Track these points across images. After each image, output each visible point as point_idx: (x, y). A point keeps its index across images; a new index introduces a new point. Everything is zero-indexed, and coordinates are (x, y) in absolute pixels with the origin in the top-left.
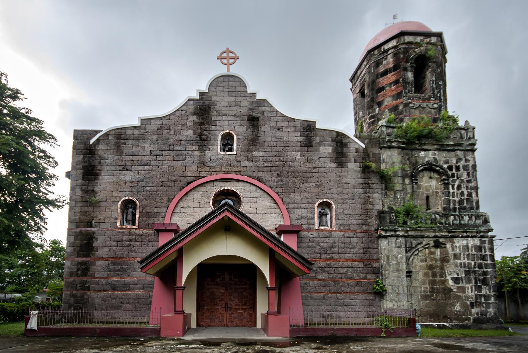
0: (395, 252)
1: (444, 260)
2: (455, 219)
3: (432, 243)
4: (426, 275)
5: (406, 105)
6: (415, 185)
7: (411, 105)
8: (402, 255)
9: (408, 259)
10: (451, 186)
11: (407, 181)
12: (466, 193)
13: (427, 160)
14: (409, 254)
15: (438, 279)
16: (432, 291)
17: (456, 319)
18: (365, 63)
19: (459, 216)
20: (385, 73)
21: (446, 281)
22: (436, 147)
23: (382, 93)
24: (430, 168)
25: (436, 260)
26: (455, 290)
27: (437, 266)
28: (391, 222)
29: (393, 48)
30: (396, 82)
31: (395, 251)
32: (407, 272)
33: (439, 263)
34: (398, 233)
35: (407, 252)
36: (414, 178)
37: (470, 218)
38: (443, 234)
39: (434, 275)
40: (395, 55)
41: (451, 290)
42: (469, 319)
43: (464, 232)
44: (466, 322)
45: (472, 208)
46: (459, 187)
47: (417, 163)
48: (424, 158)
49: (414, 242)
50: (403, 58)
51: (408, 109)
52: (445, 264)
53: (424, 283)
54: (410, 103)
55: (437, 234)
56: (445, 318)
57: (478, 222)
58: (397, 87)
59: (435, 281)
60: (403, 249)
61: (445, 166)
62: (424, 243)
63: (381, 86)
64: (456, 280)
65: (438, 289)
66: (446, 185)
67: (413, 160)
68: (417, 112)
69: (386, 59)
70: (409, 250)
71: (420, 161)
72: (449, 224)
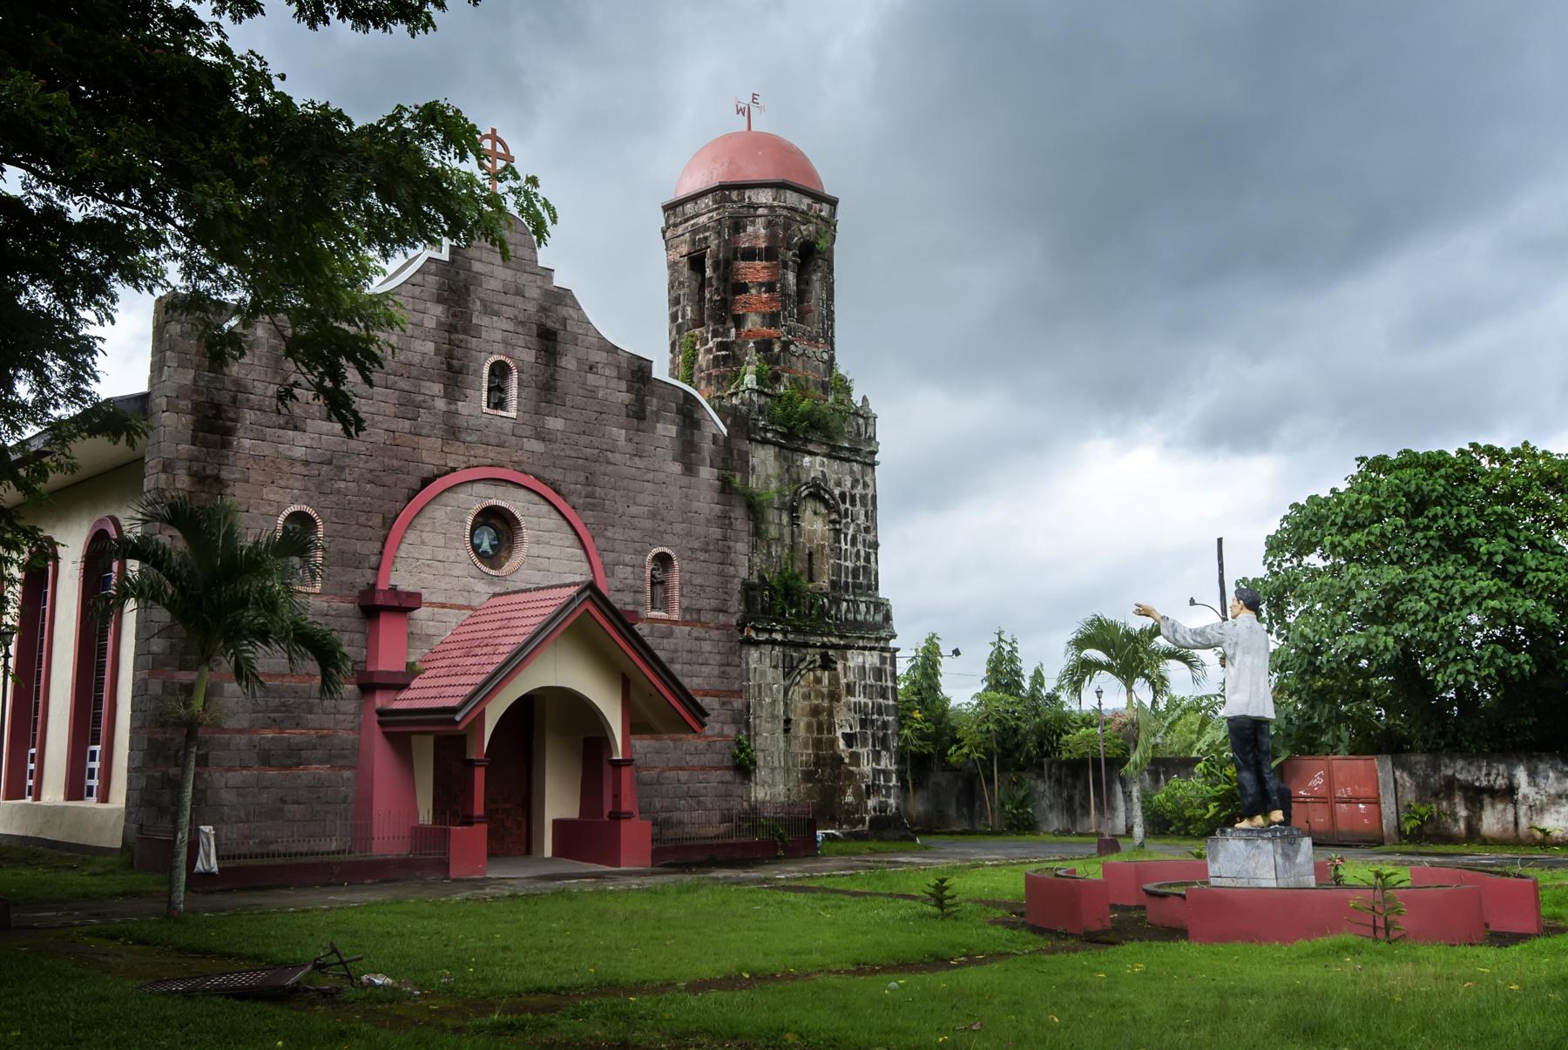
0: (769, 680)
1: (834, 696)
2: (848, 610)
4: (809, 727)
11: (785, 519)
12: (862, 553)
15: (825, 736)
16: (818, 761)
18: (708, 201)
20: (750, 255)
22: (824, 449)
23: (742, 297)
24: (818, 492)
30: (770, 287)
31: (770, 672)
33: (826, 704)
35: (786, 675)
38: (833, 640)
39: (820, 730)
40: (770, 225)
42: (862, 820)
45: (869, 587)
46: (854, 539)
47: (799, 480)
53: (806, 747)
54: (791, 342)
58: (772, 299)
61: (837, 492)
64: (849, 739)
69: (753, 223)
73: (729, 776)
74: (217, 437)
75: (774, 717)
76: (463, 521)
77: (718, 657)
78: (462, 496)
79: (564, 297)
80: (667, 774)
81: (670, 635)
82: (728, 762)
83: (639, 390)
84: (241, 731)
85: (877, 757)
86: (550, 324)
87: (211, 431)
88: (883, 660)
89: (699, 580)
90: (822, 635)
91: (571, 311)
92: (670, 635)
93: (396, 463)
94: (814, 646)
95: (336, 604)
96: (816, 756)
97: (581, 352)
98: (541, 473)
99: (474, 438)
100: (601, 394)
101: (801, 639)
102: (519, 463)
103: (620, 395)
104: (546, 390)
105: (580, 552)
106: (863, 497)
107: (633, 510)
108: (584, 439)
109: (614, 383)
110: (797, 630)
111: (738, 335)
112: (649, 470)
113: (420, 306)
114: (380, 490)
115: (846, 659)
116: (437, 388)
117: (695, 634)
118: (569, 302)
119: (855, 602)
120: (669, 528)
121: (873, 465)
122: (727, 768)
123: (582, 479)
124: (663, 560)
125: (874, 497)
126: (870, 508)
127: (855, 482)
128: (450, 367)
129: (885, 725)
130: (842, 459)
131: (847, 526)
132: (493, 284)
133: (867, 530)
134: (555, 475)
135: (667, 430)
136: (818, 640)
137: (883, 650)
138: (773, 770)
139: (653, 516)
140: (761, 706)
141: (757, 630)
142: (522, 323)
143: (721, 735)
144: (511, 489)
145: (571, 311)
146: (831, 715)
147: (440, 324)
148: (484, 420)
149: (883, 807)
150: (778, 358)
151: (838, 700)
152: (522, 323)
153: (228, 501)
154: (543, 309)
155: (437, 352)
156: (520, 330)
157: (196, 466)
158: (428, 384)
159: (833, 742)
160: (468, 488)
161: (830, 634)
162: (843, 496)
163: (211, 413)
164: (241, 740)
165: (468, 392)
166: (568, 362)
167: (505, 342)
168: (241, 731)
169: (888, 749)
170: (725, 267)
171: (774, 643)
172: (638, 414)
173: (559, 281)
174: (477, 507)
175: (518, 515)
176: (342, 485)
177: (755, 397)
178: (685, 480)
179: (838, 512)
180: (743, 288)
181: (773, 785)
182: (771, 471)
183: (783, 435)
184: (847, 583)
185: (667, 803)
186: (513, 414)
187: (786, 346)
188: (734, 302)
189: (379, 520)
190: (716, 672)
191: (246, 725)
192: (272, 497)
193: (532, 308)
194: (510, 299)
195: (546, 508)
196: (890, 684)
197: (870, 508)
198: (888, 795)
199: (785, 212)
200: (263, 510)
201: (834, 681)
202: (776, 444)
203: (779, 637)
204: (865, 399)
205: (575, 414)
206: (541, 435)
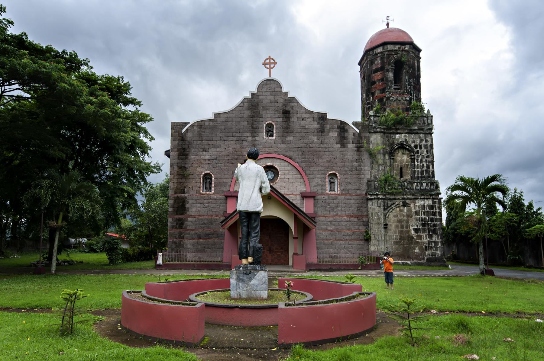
0: (377, 211)
2: (417, 185)
3: (401, 204)
4: (397, 227)
5: (388, 99)
6: (392, 160)
7: (391, 98)
8: (381, 213)
9: (385, 215)
10: (416, 160)
11: (387, 157)
12: (425, 165)
13: (400, 140)
14: (386, 212)
15: (405, 229)
17: (416, 259)
19: (420, 183)
20: (376, 71)
21: (410, 231)
22: (406, 131)
23: (374, 86)
24: (402, 146)
25: (404, 216)
26: (415, 238)
27: (404, 220)
28: (375, 188)
29: (380, 53)
30: (382, 80)
31: (377, 209)
32: (384, 225)
34: (379, 196)
35: (385, 210)
36: (391, 154)
37: (427, 185)
38: (409, 197)
39: (402, 227)
40: (382, 59)
41: (413, 238)
42: (424, 259)
43: (422, 195)
44: (422, 261)
45: (429, 177)
47: (394, 143)
48: (399, 139)
49: (390, 202)
50: (386, 62)
51: (389, 101)
52: (409, 218)
53: (395, 233)
54: (390, 97)
55: (405, 196)
56: (409, 258)
57: (432, 187)
59: (403, 231)
60: (382, 208)
61: (413, 145)
62: (396, 203)
63: (373, 80)
64: (416, 231)
65: (404, 237)
66: (413, 160)
67: (391, 141)
68: (395, 104)
69: (377, 60)
70: (386, 209)
71: (396, 142)
72: (413, 189)
73: (362, 243)
75: (379, 223)
77: (357, 205)
79: (293, 99)
80: (336, 242)
81: (336, 198)
82: (362, 237)
85: (431, 236)
86: (287, 109)
87: (183, 155)
88: (434, 203)
89: (348, 181)
90: (403, 195)
92: (336, 198)
94: (399, 199)
95: (219, 196)
96: (401, 236)
97: (299, 115)
98: (285, 153)
100: (307, 127)
101: (392, 197)
103: (315, 126)
104: (287, 129)
105: (299, 176)
106: (426, 146)
107: (321, 161)
109: (312, 123)
110: (389, 194)
111: (373, 99)
112: (326, 148)
113: (242, 112)
114: (231, 165)
115: (416, 203)
116: (249, 134)
117: (347, 197)
118: (294, 101)
119: (420, 183)
120: (335, 165)
121: (431, 134)
122: (362, 240)
123: (300, 153)
124: (335, 175)
125: (432, 145)
126: (429, 149)
127: (421, 141)
128: (253, 128)
129: (435, 225)
130: (415, 133)
131: (418, 156)
132: (267, 101)
133: (428, 157)
134: (291, 153)
135: (334, 134)
136: (401, 197)
137: (433, 199)
138: (378, 241)
139: (329, 162)
140: (373, 220)
141: (371, 195)
142: (277, 111)
143: (358, 229)
145: (295, 104)
146: (407, 222)
147: (249, 116)
149: (433, 255)
150: (385, 102)
151: (411, 217)
152: (277, 111)
154: (285, 105)
155: (248, 124)
156: (276, 113)
157: (179, 165)
159: (409, 231)
161: (406, 194)
162: (416, 147)
163: (182, 151)
164: (193, 232)
165: (260, 134)
166: (294, 119)
167: (271, 117)
169: (436, 234)
170: (369, 76)
171: (378, 199)
172: (322, 131)
173: (290, 96)
175: (277, 167)
177: (372, 118)
178: (342, 149)
179: (413, 152)
180: (374, 83)
181: (379, 245)
182: (379, 142)
183: (384, 129)
184: (418, 177)
185: (336, 251)
186: (274, 138)
187: (388, 99)
188: (372, 88)
190: (356, 209)
193: (280, 105)
194: (273, 104)
195: (287, 164)
196: (437, 210)
197: (429, 149)
198: (437, 251)
199: (387, 53)
201: (410, 211)
202: (381, 132)
203: (381, 197)
204: (428, 110)
205: (297, 134)
206: (284, 143)
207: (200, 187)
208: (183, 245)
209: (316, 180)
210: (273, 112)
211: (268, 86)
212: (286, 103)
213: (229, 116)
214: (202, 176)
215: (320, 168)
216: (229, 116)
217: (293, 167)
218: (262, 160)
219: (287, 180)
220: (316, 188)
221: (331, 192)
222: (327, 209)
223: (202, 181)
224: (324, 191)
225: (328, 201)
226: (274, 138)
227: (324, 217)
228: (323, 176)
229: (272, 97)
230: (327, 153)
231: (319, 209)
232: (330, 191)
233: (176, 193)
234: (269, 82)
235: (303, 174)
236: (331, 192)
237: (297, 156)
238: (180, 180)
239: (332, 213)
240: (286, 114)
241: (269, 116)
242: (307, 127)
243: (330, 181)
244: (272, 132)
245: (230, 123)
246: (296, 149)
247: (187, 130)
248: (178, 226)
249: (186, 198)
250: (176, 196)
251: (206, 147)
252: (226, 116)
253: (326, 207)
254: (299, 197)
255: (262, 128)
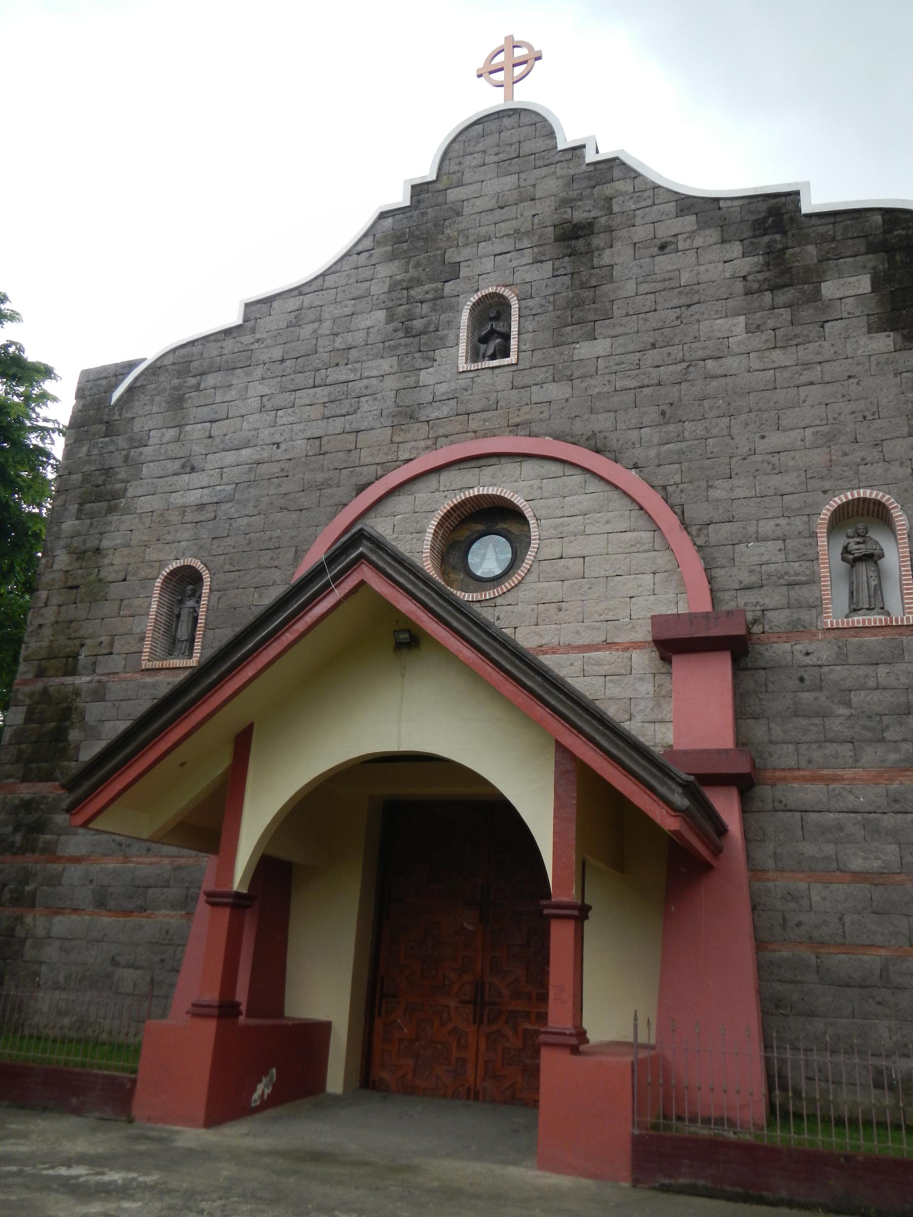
74: (104, 504)
76: (423, 531)
78: (422, 494)
79: (613, 167)
83: (769, 245)
84: (77, 860)
86: (579, 216)
87: (99, 498)
91: (625, 186)
93: (320, 477)
97: (640, 233)
99: (445, 410)
102: (527, 423)
103: (726, 263)
104: (582, 305)
105: (646, 536)
107: (776, 440)
108: (653, 356)
112: (807, 365)
113: (366, 273)
114: (294, 516)
120: (875, 454)
123: (653, 414)
124: (877, 513)
128: (408, 333)
132: (480, 204)
134: (602, 422)
139: (830, 439)
144: (509, 467)
148: (463, 382)
153: (103, 574)
154: (567, 202)
155: (390, 318)
156: (526, 243)
157: (76, 542)
158: (373, 364)
160: (432, 482)
166: (618, 256)
168: (77, 860)
174: (447, 505)
175: (519, 501)
176: (244, 521)
189: (290, 555)
191: (84, 851)
192: (154, 557)
195: (578, 478)
200: (143, 574)
206: (563, 375)
207: (142, 639)
208: (23, 941)
209: (750, 553)
210: (508, 244)
211: (491, 140)
212: (573, 194)
213: (307, 300)
214: (158, 583)
215: (776, 481)
216: (307, 300)
217: (615, 495)
218: (446, 478)
219: (576, 566)
220: (750, 597)
221: (858, 620)
222: (835, 726)
223: (154, 606)
224: (806, 616)
225: (839, 672)
226: (512, 359)
227: (814, 779)
228: (799, 523)
229: (510, 181)
230: (815, 393)
231: (777, 732)
232: (855, 610)
233: (41, 673)
234: (493, 126)
235: (668, 521)
236: (858, 620)
237: (634, 435)
238: (69, 612)
239: (871, 755)
240: (574, 238)
241: (488, 264)
242: (685, 278)
243: (846, 550)
244: (506, 337)
245: (306, 331)
246: (629, 397)
247: (130, 389)
248: (18, 838)
249: (77, 693)
250: (39, 685)
251: (196, 448)
252: (293, 304)
253: (825, 715)
254: (644, 660)
255: (452, 324)
